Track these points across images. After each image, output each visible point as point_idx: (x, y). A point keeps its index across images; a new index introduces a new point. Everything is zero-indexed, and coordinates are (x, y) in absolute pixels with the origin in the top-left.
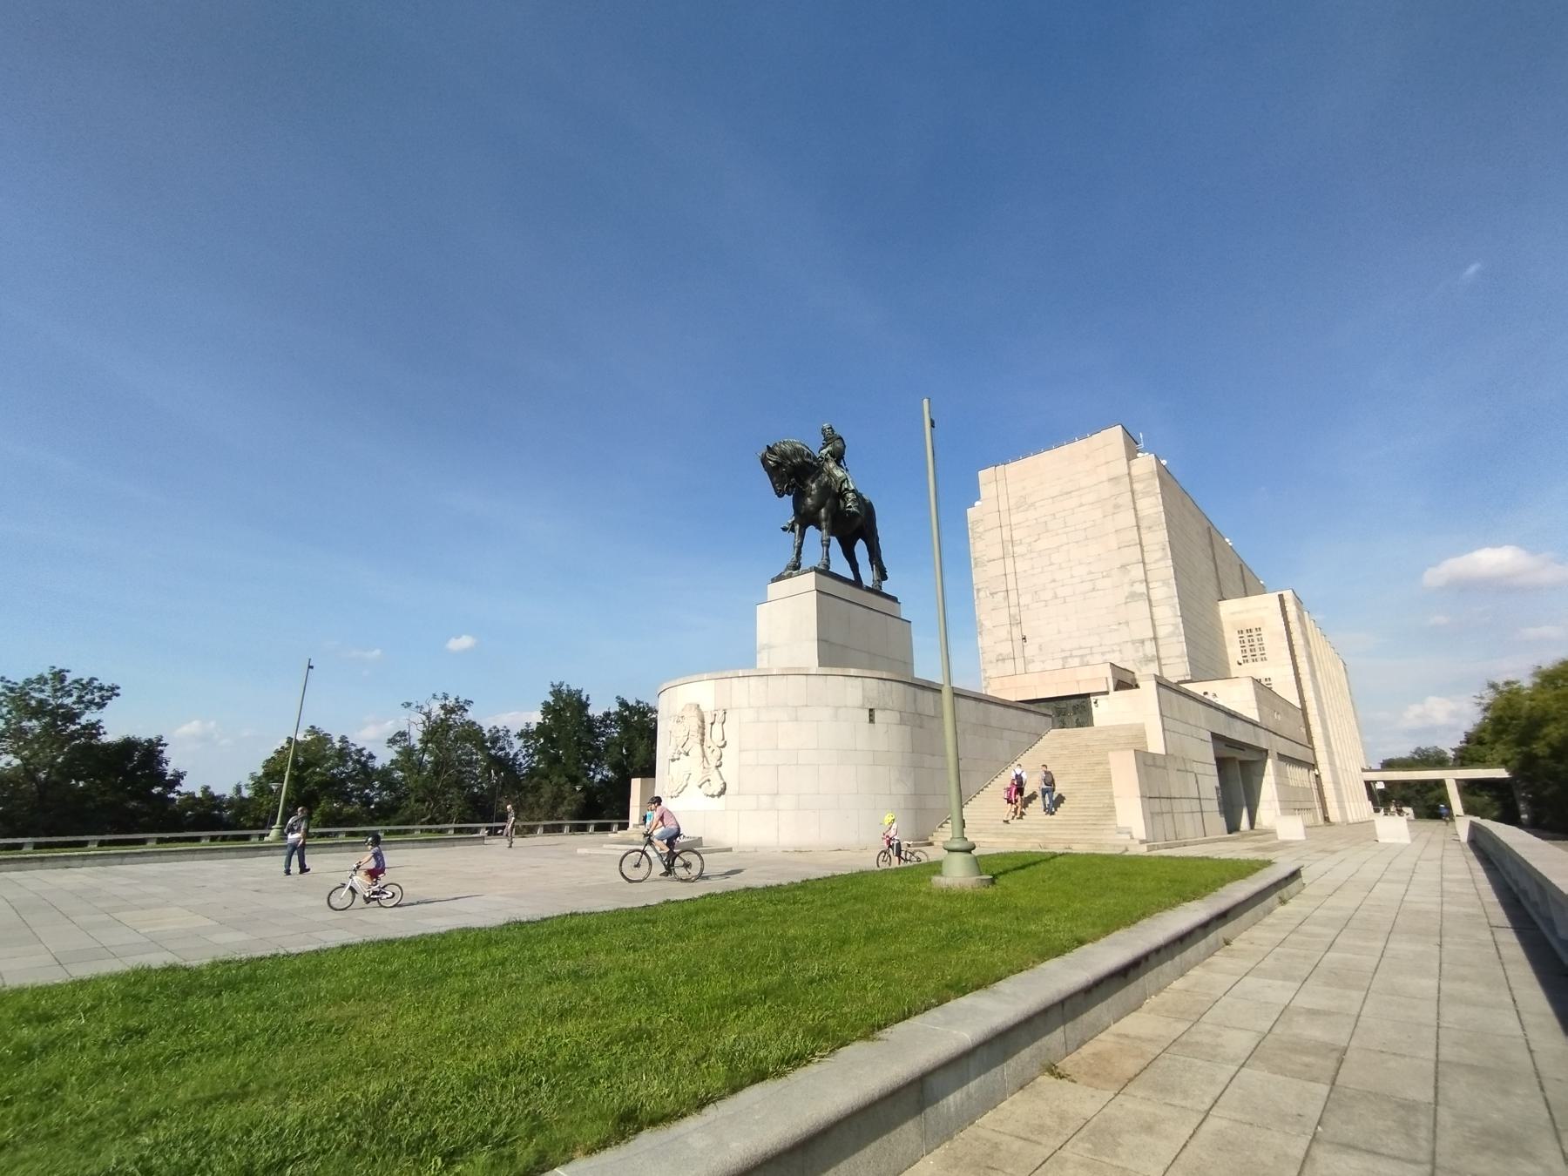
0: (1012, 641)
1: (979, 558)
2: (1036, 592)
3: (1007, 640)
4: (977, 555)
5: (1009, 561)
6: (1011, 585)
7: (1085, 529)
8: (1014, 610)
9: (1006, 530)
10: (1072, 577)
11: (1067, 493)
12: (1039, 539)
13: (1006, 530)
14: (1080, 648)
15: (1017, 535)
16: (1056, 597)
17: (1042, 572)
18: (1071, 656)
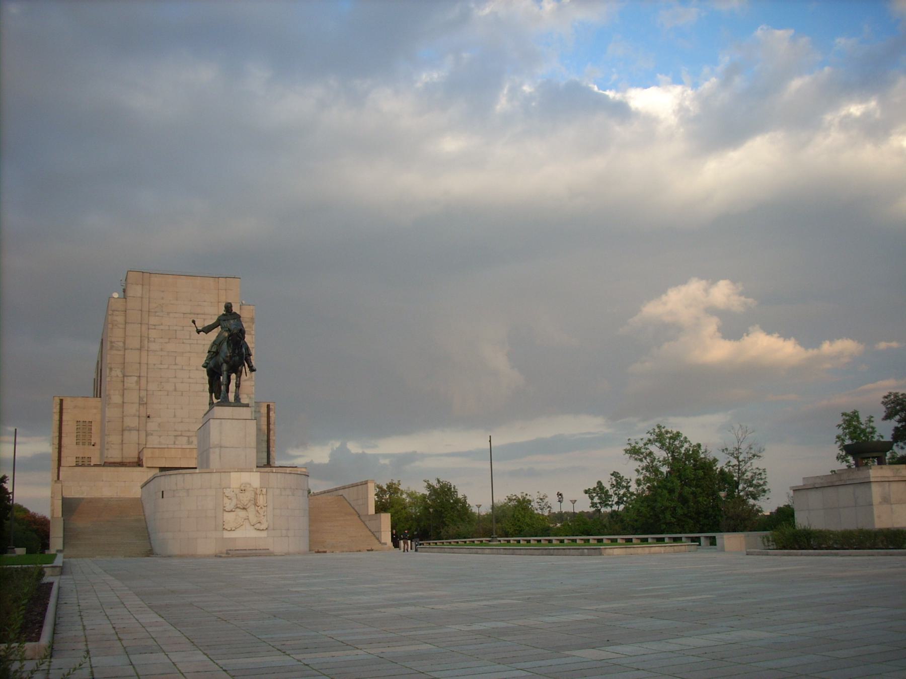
0: (139, 417)
1: (114, 342)
2: (161, 382)
3: (134, 416)
4: (113, 340)
5: (144, 354)
6: (143, 373)
7: (204, 345)
8: (143, 393)
9: (144, 327)
10: (190, 378)
11: (195, 314)
12: (169, 342)
13: (144, 327)
14: (189, 431)
15: (153, 334)
16: (175, 390)
17: (168, 368)
18: (181, 435)
